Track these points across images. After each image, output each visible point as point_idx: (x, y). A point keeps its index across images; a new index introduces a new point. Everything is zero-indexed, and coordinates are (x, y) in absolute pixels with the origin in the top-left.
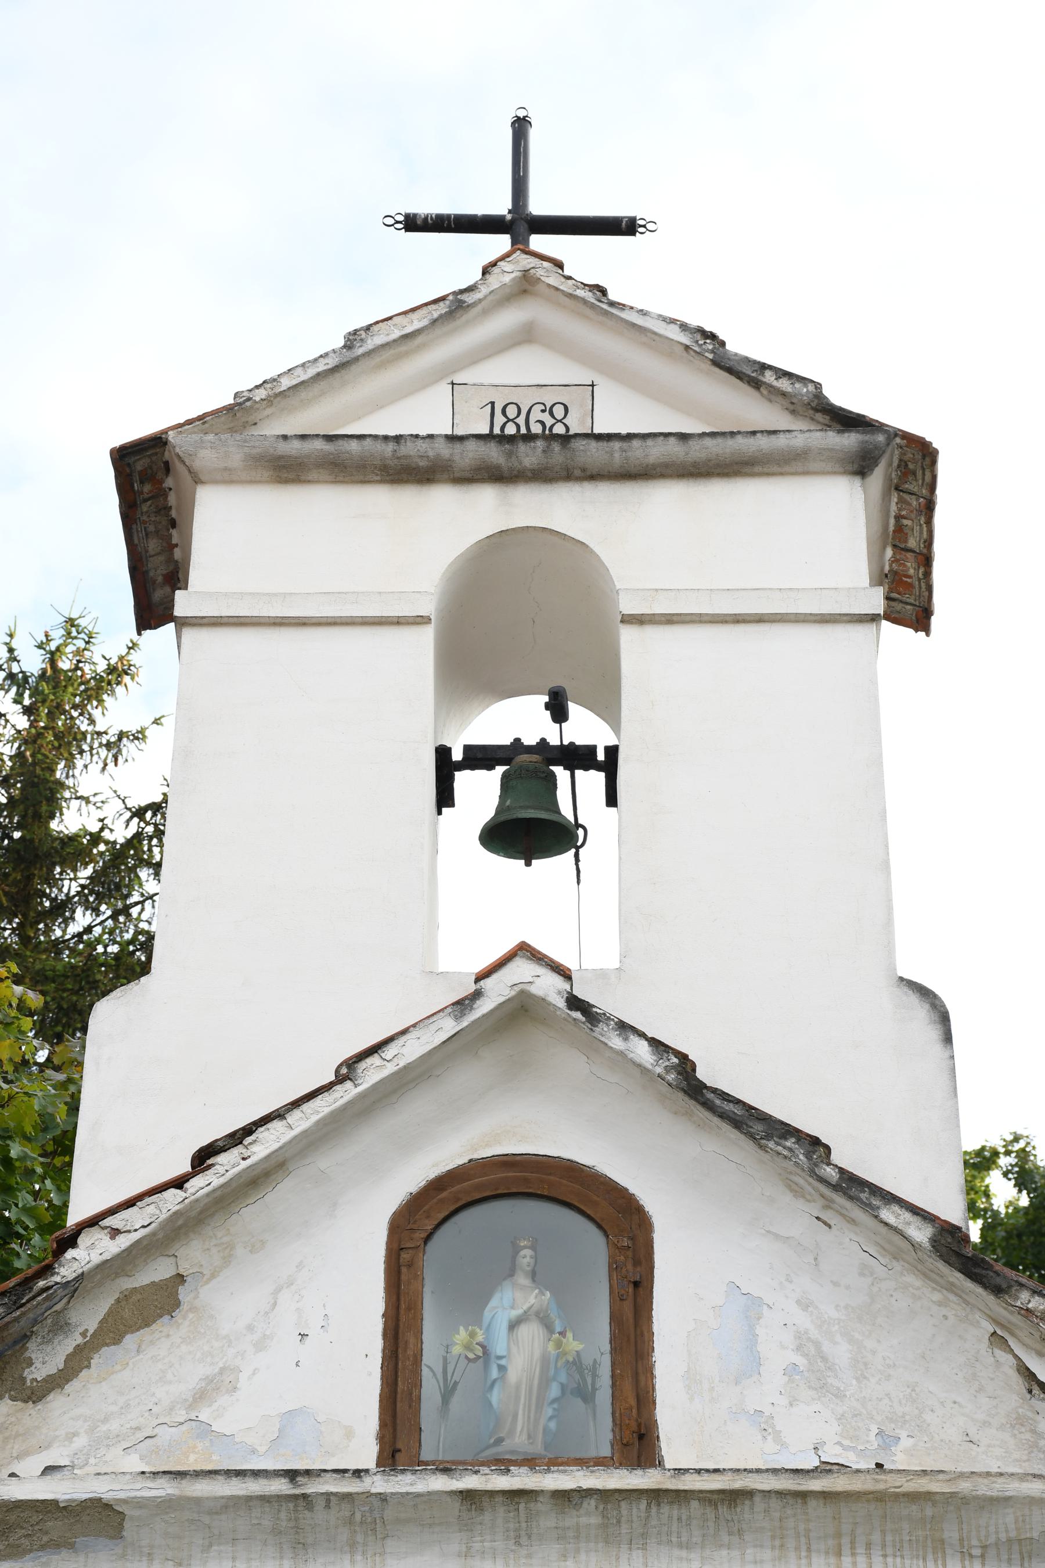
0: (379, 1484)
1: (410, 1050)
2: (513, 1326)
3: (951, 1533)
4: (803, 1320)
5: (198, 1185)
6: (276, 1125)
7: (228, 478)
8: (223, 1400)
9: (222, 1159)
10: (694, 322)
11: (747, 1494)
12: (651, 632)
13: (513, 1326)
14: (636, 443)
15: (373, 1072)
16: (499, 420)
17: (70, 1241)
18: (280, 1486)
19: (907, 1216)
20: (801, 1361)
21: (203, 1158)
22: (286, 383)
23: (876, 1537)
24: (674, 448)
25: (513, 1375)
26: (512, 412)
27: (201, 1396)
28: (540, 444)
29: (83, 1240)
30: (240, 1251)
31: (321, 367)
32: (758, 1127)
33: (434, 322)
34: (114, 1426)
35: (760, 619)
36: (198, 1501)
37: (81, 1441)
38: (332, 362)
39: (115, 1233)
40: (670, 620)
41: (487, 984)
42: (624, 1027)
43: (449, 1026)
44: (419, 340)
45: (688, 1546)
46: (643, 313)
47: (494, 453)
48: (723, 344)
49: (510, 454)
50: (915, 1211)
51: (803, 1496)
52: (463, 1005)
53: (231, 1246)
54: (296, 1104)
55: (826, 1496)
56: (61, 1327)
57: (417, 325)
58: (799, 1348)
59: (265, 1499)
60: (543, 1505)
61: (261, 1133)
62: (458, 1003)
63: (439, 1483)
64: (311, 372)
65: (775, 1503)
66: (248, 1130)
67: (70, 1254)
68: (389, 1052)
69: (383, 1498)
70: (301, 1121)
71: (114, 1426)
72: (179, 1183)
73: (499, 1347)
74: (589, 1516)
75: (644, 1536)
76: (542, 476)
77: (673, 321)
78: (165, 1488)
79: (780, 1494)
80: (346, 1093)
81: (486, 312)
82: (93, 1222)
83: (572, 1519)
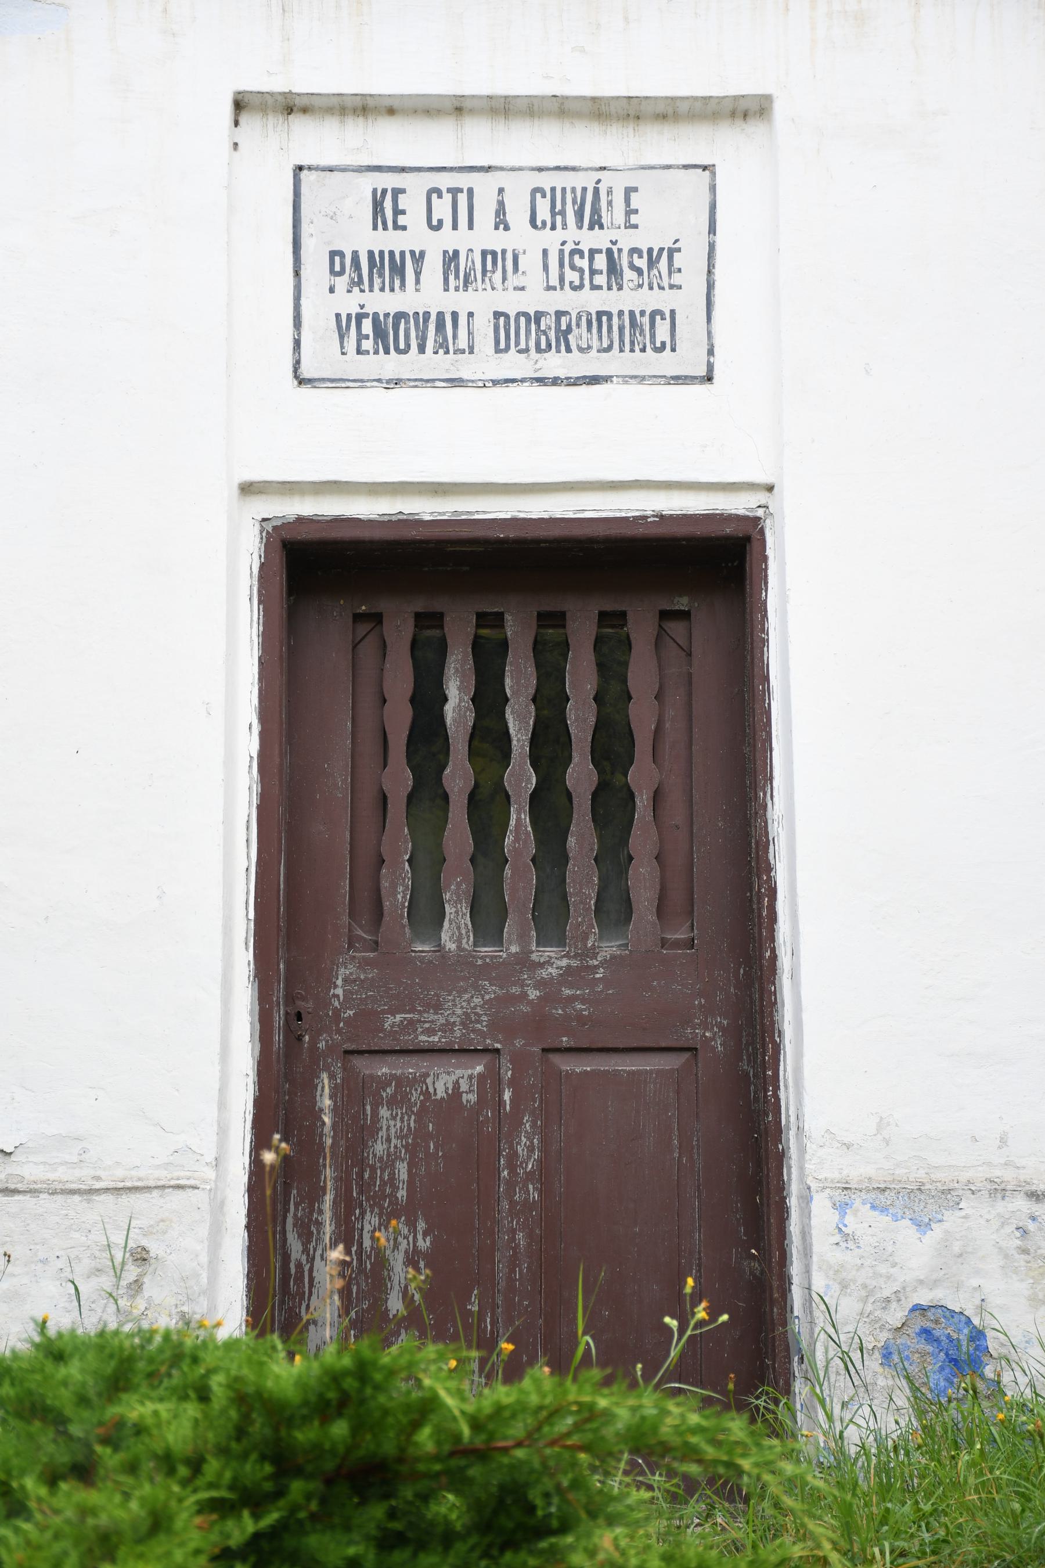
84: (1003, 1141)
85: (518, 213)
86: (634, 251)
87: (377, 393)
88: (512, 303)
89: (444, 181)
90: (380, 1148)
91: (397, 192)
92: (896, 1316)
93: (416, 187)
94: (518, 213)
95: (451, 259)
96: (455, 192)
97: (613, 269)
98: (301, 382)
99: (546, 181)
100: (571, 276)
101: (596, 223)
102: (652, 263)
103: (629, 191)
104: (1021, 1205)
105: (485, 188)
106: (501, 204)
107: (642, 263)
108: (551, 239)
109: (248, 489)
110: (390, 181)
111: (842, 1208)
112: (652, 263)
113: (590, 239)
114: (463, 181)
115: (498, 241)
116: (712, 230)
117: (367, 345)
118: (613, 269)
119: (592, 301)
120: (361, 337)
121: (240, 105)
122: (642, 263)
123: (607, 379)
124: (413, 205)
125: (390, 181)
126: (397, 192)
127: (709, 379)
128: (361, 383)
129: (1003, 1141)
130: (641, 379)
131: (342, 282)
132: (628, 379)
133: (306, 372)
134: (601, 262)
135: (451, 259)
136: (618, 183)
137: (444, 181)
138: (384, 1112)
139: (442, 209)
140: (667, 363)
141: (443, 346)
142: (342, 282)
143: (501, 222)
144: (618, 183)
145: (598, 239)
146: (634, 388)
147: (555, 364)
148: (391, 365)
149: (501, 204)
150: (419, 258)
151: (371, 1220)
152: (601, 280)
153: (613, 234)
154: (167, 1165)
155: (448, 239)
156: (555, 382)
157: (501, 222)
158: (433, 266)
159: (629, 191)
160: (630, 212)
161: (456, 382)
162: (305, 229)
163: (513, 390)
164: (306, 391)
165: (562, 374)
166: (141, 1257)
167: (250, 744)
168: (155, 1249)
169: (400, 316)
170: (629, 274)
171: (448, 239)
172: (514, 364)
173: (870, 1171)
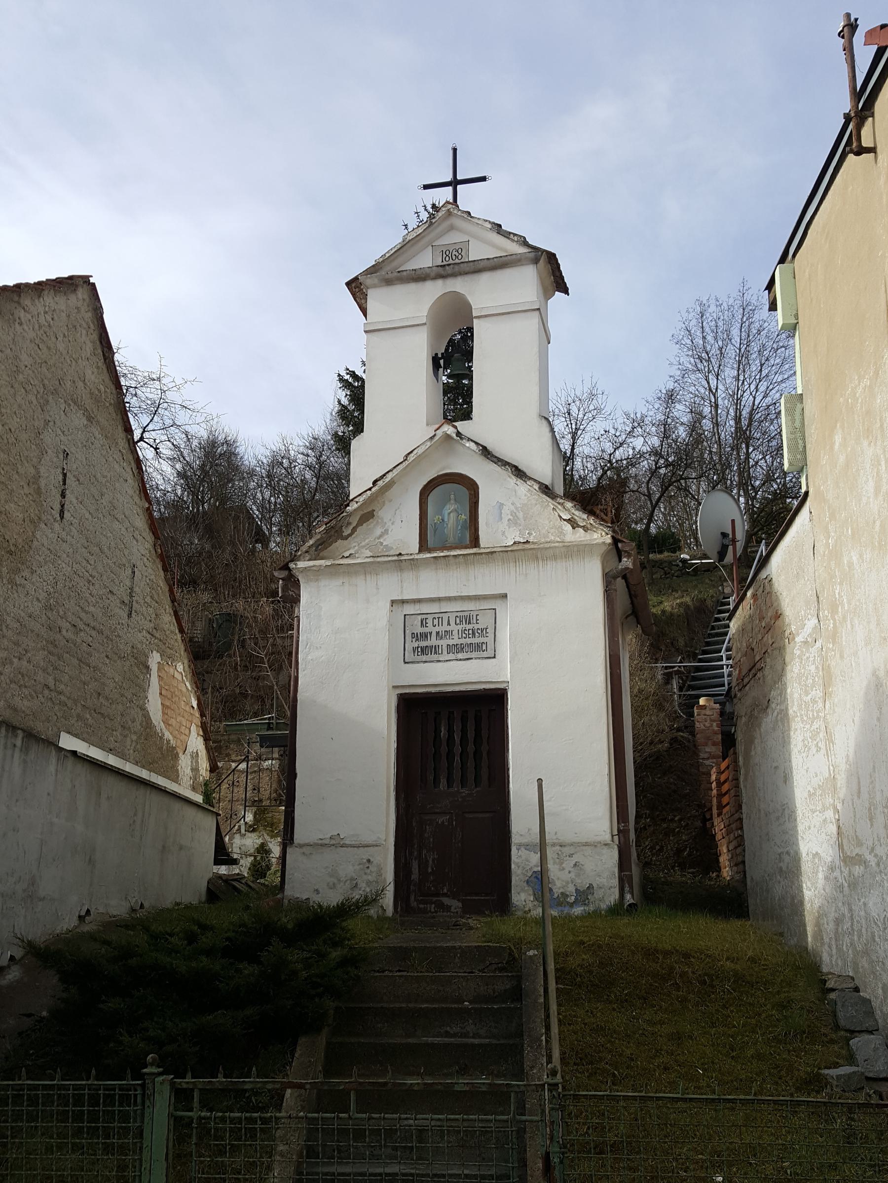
0: (416, 557)
1: (420, 451)
2: (449, 514)
3: (539, 556)
4: (512, 508)
5: (373, 490)
6: (390, 473)
7: (375, 286)
8: (386, 537)
9: (379, 483)
10: (492, 220)
11: (495, 552)
12: (482, 320)
13: (449, 514)
14: (476, 263)
15: (412, 458)
16: (444, 255)
17: (348, 505)
18: (396, 558)
19: (533, 482)
20: (511, 518)
21: (375, 483)
22: (387, 255)
23: (523, 558)
24: (486, 263)
25: (449, 526)
26: (447, 254)
27: (380, 536)
28: (452, 266)
29: (350, 505)
30: (386, 502)
31: (396, 249)
32: (500, 463)
33: (424, 230)
34: (363, 544)
35: (509, 313)
36: (379, 562)
37: (356, 548)
38: (399, 247)
39: (357, 502)
40: (486, 316)
41: (438, 431)
42: (469, 440)
43: (429, 444)
44: (422, 235)
45: (483, 564)
46: (479, 219)
47: (440, 270)
48: (500, 226)
49: (444, 270)
50: (535, 481)
51: (507, 551)
52: (432, 438)
53: (384, 502)
54: (395, 467)
55: (511, 551)
56: (349, 524)
57: (420, 231)
58: (511, 515)
59: (392, 561)
60: (451, 558)
61: (387, 475)
62: (431, 438)
63: (428, 555)
64: (394, 251)
65: (501, 553)
66: (384, 475)
67: (348, 508)
68: (415, 452)
69: (417, 559)
70: (395, 472)
71: (363, 544)
72: (370, 489)
73: (446, 520)
74: (461, 559)
75: (474, 562)
76: (454, 275)
77: (487, 221)
78: (371, 560)
79: (502, 551)
80: (407, 463)
81: (439, 224)
82: (352, 500)
83: (457, 560)
84: (556, 833)
85: (452, 622)
86: (478, 629)
87: (422, 664)
88: (451, 642)
89: (436, 616)
90: (426, 835)
91: (426, 619)
92: (529, 874)
93: (430, 617)
94: (452, 622)
95: (438, 633)
96: (439, 618)
97: (473, 633)
98: (405, 663)
99: (459, 614)
100: (464, 635)
101: (470, 623)
102: (482, 631)
103: (477, 615)
104: (558, 848)
105: (445, 616)
106: (449, 620)
107: (480, 632)
108: (460, 627)
109: (394, 687)
110: (424, 616)
111: (518, 849)
112: (482, 631)
113: (470, 626)
114: (440, 615)
115: (448, 628)
116: (495, 623)
117: (419, 654)
118: (473, 633)
119: (469, 641)
120: (418, 652)
121: (393, 602)
122: (480, 632)
123: (472, 659)
124: (430, 622)
125: (424, 616)
126: (426, 619)
127: (494, 657)
128: (418, 662)
129: (556, 833)
130: (479, 658)
131: (414, 640)
132: (476, 658)
133: (406, 661)
134: (471, 632)
135: (438, 633)
136: (475, 614)
137: (436, 616)
138: (427, 827)
139: (436, 622)
140: (485, 654)
141: (435, 653)
142: (414, 640)
143: (449, 624)
144: (475, 614)
145: (470, 626)
146: (478, 660)
147: (460, 656)
148: (424, 658)
149: (449, 620)
150: (431, 633)
151: (424, 852)
152: (470, 636)
153: (473, 625)
154: (376, 841)
155: (437, 629)
156: (460, 660)
157: (449, 624)
158: (434, 634)
159: (477, 615)
160: (477, 620)
161: (439, 661)
162: (407, 628)
163: (452, 663)
164: (406, 665)
165: (462, 658)
166: (369, 861)
167: (394, 745)
168: (372, 860)
169: (427, 646)
170: (477, 634)
171: (437, 629)
172: (451, 656)
173: (526, 841)
